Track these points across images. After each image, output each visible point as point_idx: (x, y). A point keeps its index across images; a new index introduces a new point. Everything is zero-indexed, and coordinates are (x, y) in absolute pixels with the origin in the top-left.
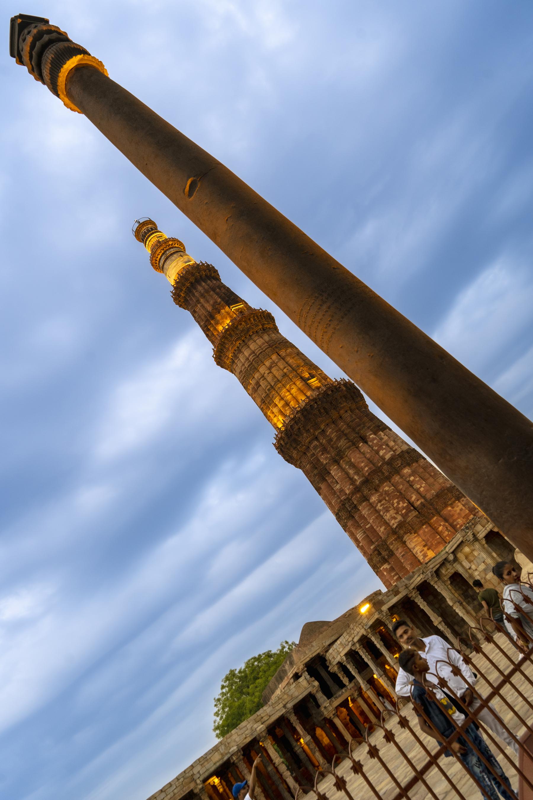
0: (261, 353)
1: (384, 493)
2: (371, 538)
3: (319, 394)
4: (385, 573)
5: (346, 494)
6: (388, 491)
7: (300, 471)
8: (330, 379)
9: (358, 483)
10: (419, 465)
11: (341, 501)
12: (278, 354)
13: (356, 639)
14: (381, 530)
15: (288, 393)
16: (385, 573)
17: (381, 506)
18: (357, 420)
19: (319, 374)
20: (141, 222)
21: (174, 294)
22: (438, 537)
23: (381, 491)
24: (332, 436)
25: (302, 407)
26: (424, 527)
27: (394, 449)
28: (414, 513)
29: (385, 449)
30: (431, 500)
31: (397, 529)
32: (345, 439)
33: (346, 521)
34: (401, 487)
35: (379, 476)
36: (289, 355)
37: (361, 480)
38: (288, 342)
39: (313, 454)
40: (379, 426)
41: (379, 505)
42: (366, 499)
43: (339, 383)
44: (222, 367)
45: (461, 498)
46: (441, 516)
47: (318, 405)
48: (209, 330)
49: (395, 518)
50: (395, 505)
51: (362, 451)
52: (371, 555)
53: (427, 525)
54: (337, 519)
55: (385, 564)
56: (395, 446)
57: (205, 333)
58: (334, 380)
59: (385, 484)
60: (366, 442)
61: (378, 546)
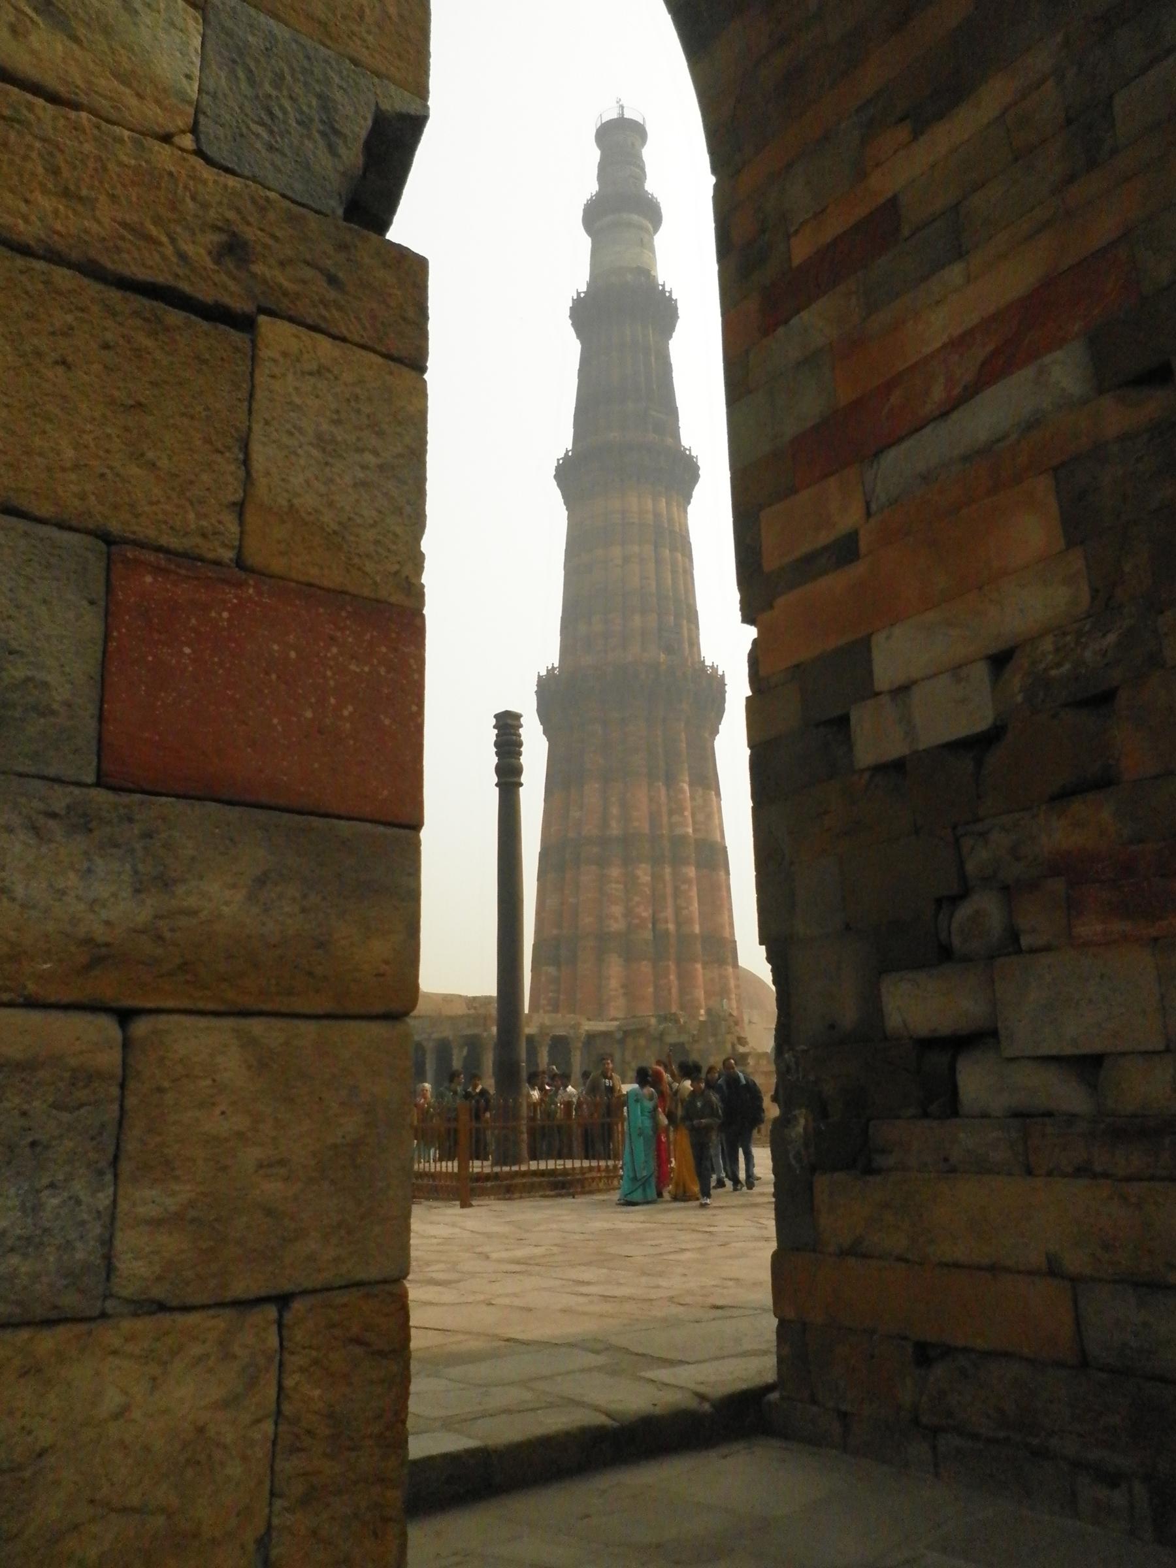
4: (543, 979)
6: (638, 878)
7: (546, 744)
12: (656, 547)
13: (435, 1036)
14: (587, 921)
16: (543, 979)
22: (651, 990)
26: (645, 963)
28: (648, 935)
41: (614, 886)
59: (643, 865)
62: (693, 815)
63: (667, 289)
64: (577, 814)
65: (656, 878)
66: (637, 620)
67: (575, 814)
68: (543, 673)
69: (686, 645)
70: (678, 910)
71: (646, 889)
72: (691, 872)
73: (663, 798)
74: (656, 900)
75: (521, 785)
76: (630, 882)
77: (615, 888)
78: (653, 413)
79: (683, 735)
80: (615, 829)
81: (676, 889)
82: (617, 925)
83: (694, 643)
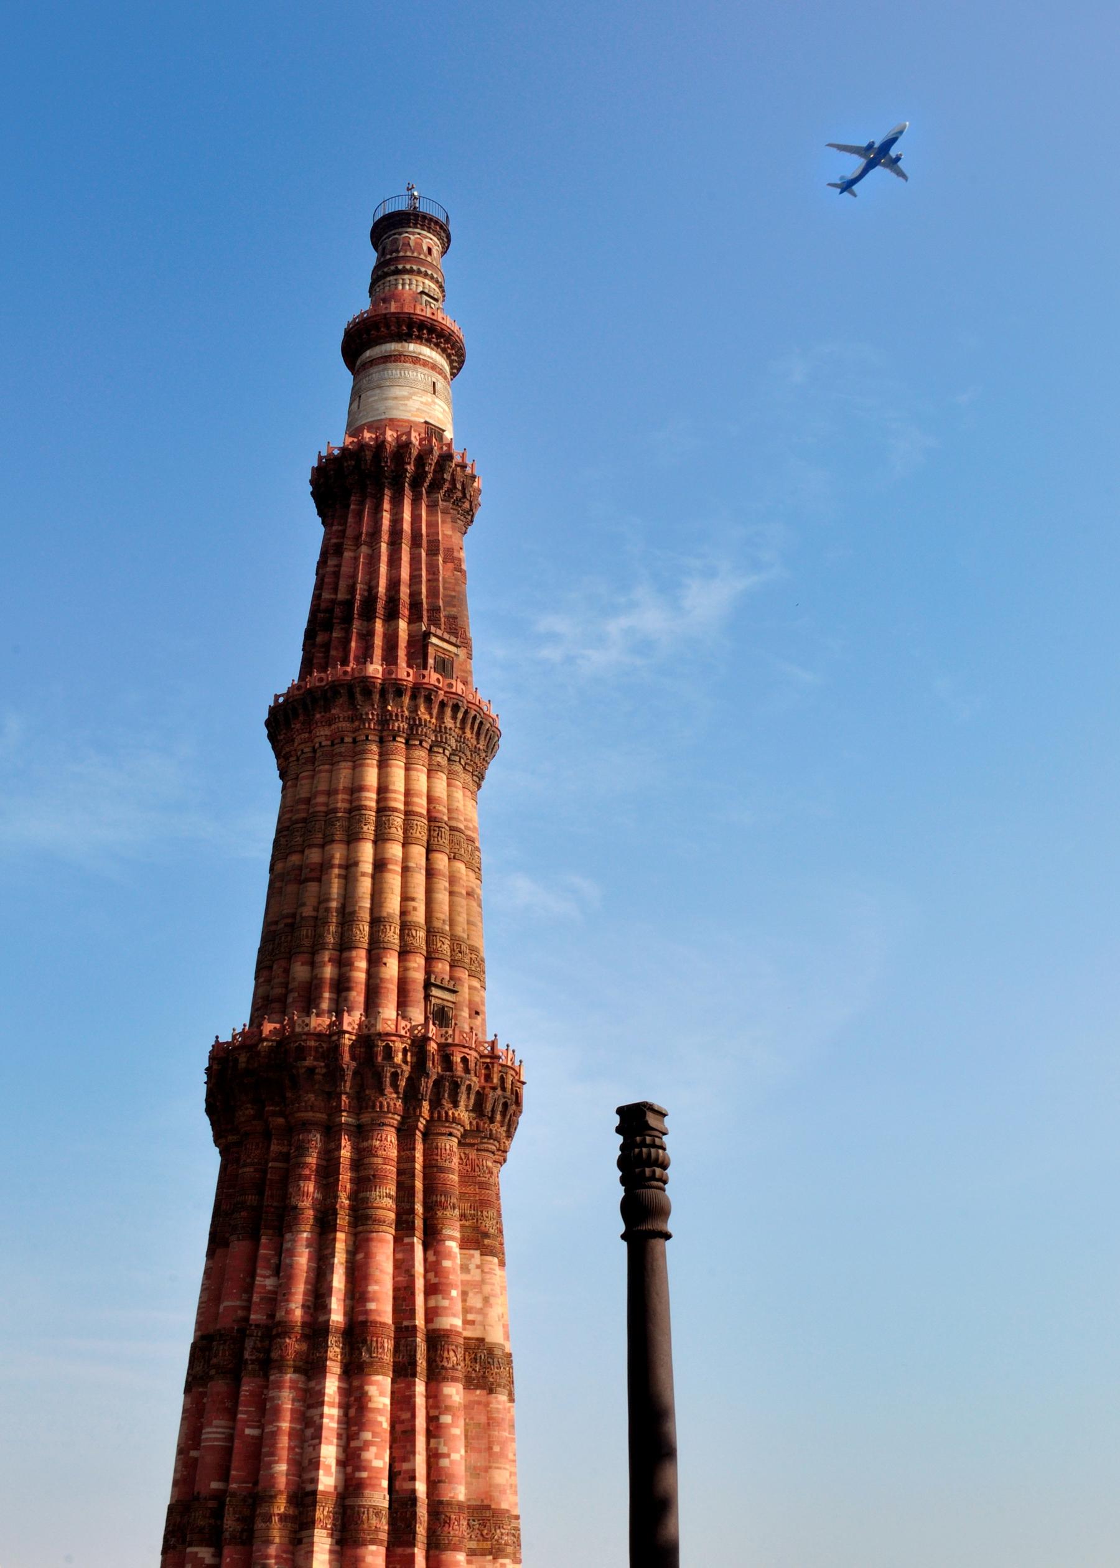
0: (395, 810)
1: (357, 1394)
2: (235, 1464)
3: (430, 1039)
5: (272, 1316)
8: (484, 1020)
9: (321, 1319)
10: (487, 1404)
11: (246, 1319)
12: (429, 851)
15: (362, 964)
18: (455, 1178)
19: (471, 988)
20: (425, 208)
23: (356, 1383)
24: (366, 1161)
25: (365, 1031)
26: (373, 1548)
27: (470, 1317)
28: (379, 1498)
29: (452, 1299)
30: (441, 1503)
31: (309, 1499)
32: (389, 1196)
33: (213, 1372)
34: (406, 1416)
35: (383, 1347)
36: (452, 880)
38: (471, 840)
39: (285, 1157)
40: (486, 1235)
43: (494, 1056)
44: (272, 737)
45: (506, 1557)
46: (427, 1558)
47: (405, 1061)
48: (328, 627)
50: (353, 1444)
51: (400, 1256)
52: (197, 1498)
53: (382, 1550)
54: (195, 1347)
55: (208, 1545)
56: (480, 1311)
57: (312, 621)
59: (379, 1378)
60: (426, 1247)
61: (233, 1495)
62: (464, 1294)
63: (469, 462)
64: (270, 1283)
65: (402, 1401)
66: (391, 967)
67: (265, 1281)
68: (226, 1038)
69: (465, 1013)
70: (433, 1457)
75: (667, 1236)
78: (434, 640)
79: (456, 1160)
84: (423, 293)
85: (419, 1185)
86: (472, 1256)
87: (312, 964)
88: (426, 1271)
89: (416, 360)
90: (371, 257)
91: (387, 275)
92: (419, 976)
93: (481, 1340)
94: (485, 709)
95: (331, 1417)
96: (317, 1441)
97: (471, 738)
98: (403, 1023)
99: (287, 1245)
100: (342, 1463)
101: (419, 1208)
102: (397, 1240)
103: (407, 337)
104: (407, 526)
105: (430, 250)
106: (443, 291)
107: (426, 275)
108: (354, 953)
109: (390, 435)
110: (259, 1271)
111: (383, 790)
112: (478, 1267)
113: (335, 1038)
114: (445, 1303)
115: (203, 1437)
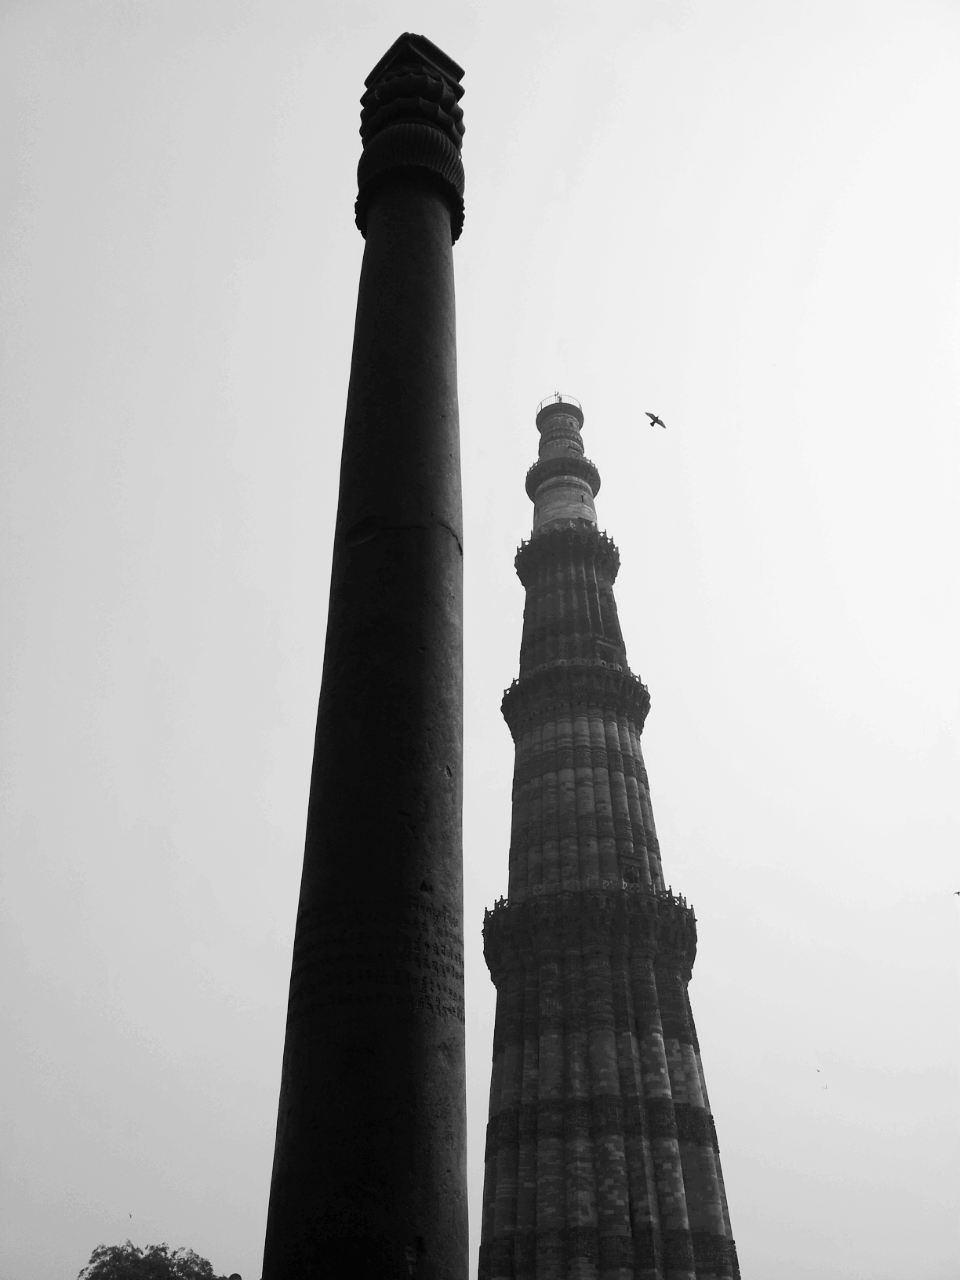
0: (586, 747)
5: (537, 1098)
6: (610, 1154)
9: (570, 1096)
15: (574, 847)
17: (576, 1168)
20: (563, 401)
21: (524, 547)
26: (624, 1270)
27: (677, 1088)
29: (661, 1075)
32: (607, 1003)
36: (630, 787)
37: (578, 1094)
41: (579, 1164)
42: (564, 1134)
43: (671, 899)
44: (506, 719)
49: (585, 1212)
50: (600, 1189)
51: (620, 1046)
58: (667, 889)
59: (615, 1137)
60: (639, 1038)
62: (671, 1072)
63: (609, 536)
65: (632, 1154)
67: (531, 1073)
68: (491, 908)
70: (661, 1197)
71: (620, 1168)
72: (674, 1146)
73: (634, 1052)
74: (634, 1184)
76: (600, 1158)
77: (582, 1168)
78: (599, 642)
80: (579, 1090)
81: (657, 1167)
82: (585, 1218)
83: (657, 874)
84: (569, 447)
85: (628, 993)
86: (674, 1044)
87: (542, 852)
88: (641, 1056)
89: (570, 485)
90: (538, 435)
91: (547, 441)
92: (613, 851)
93: (689, 1105)
94: (637, 680)
95: (584, 1169)
96: (574, 1189)
97: (632, 702)
98: (605, 882)
99: (541, 1045)
100: (595, 1205)
101: (630, 1010)
102: (618, 1035)
103: (564, 472)
104: (573, 578)
105: (571, 424)
106: (582, 446)
107: (569, 438)
108: (567, 841)
109: (557, 526)
110: (525, 1066)
111: (575, 735)
112: (678, 1051)
113: (560, 896)
114: (657, 1078)
115: (497, 1191)
